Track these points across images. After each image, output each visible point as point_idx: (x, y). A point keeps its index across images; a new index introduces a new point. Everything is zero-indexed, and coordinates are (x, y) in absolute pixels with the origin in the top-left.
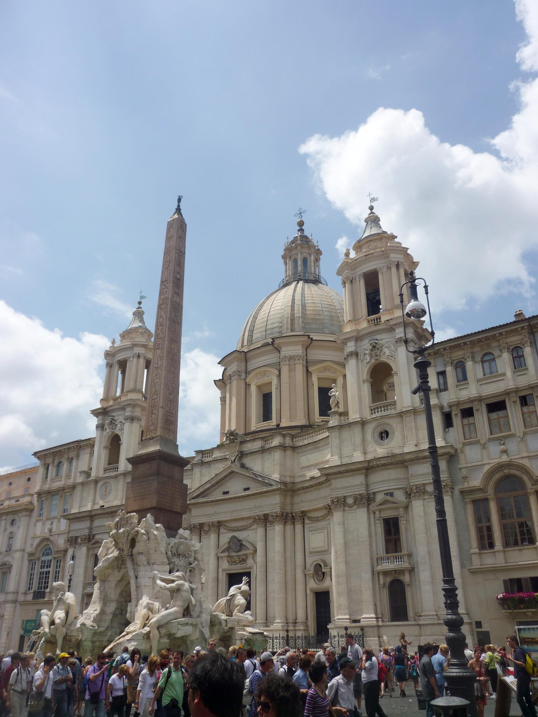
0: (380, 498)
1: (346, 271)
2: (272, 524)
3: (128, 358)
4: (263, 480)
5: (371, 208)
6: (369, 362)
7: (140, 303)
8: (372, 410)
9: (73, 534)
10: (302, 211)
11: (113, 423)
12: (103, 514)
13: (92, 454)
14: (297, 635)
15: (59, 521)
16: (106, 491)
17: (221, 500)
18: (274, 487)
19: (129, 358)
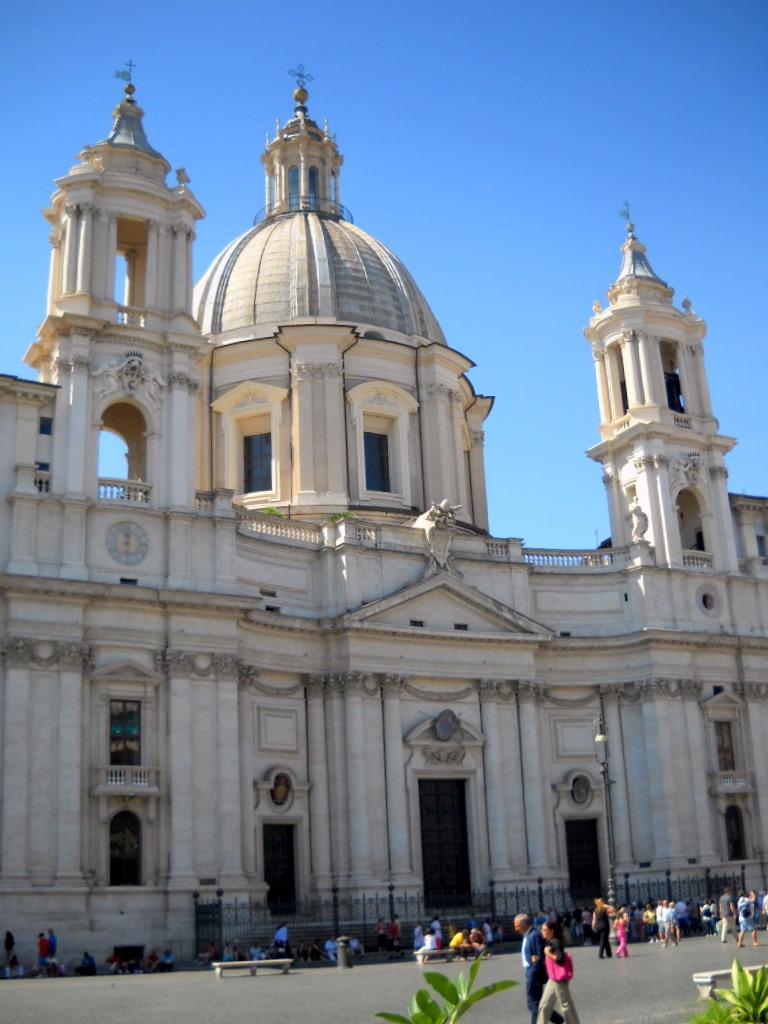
2: (507, 700)
3: (155, 222)
4: (514, 617)
6: (682, 484)
7: (130, 90)
8: (684, 558)
9: (25, 632)
10: (305, 74)
11: (133, 371)
12: (141, 601)
13: (46, 427)
14: (366, 897)
16: (127, 543)
17: (405, 635)
18: (540, 638)
19: (158, 225)
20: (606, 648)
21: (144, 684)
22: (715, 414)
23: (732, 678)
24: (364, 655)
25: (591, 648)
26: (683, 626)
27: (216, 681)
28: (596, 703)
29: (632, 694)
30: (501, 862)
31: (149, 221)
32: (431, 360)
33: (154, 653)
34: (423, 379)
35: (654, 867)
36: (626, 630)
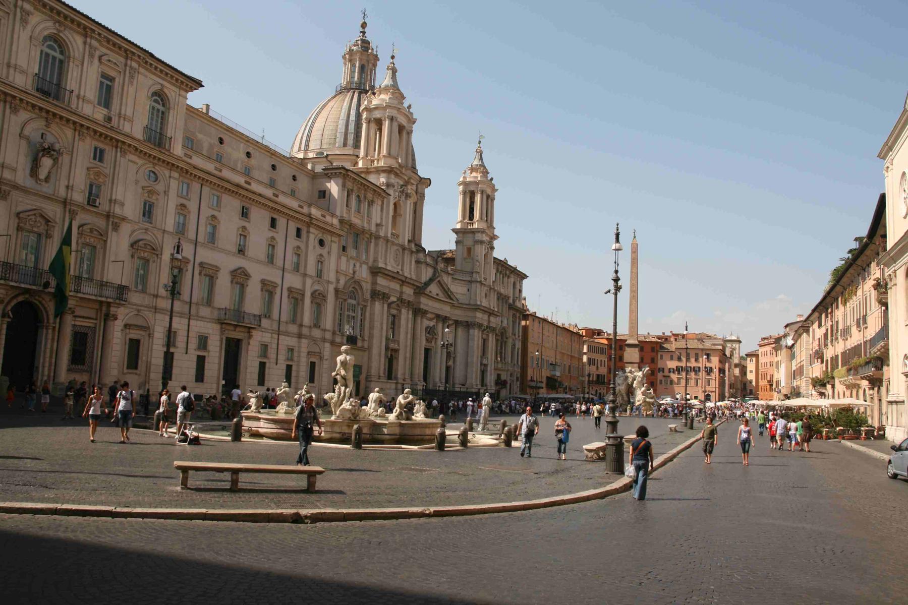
0: (483, 328)
1: (485, 186)
5: (480, 142)
15: (361, 266)
20: (462, 308)
21: (398, 310)
22: (495, 225)
23: (486, 324)
24: (425, 303)
25: (458, 307)
26: (483, 304)
27: (408, 310)
28: (454, 326)
29: (468, 325)
30: (437, 380)
31: (404, 127)
32: (423, 183)
33: (398, 300)
34: (419, 190)
35: (466, 386)
36: (467, 302)
